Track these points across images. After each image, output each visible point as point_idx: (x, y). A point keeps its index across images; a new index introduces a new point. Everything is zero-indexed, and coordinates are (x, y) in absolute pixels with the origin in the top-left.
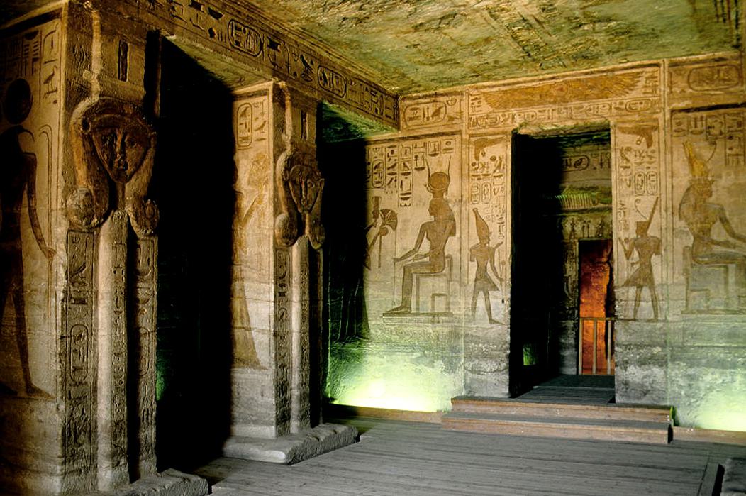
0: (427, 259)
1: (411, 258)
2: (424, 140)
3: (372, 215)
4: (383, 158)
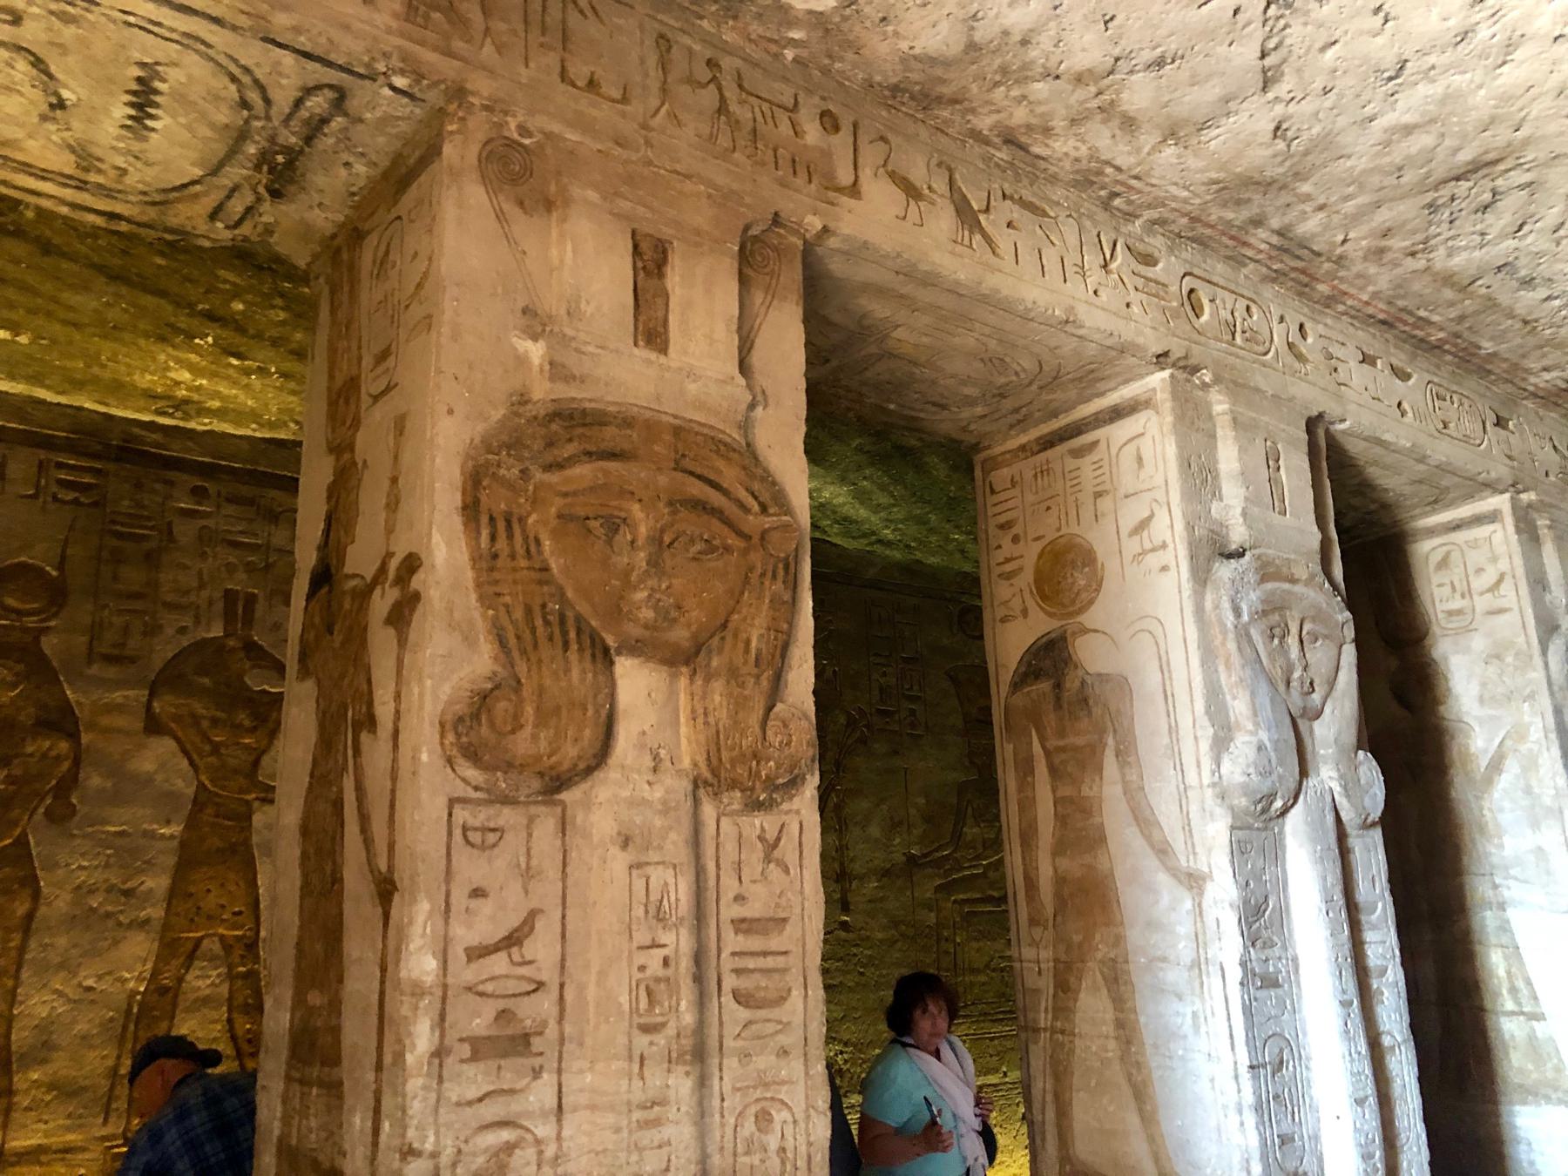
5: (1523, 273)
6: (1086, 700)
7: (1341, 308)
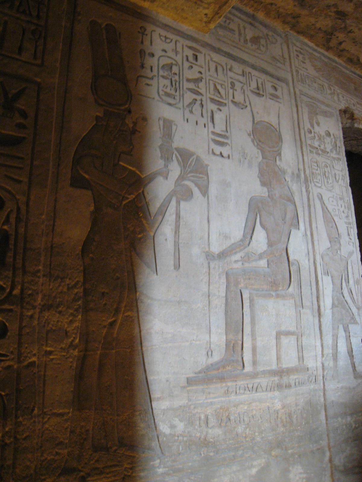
1: (237, 257)
3: (158, 153)
4: (179, 58)
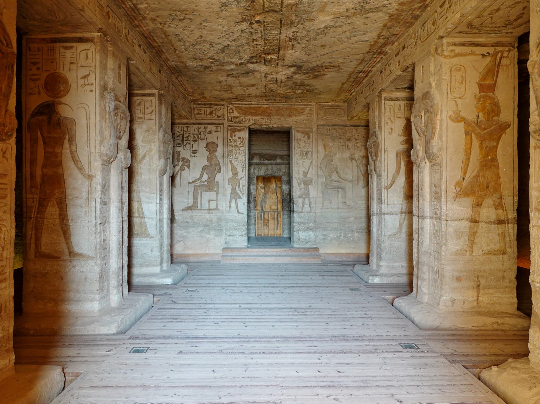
0: (206, 183)
2: (204, 126)
4: (182, 132)
5: (180, 38)
6: (60, 124)
7: (138, 29)
